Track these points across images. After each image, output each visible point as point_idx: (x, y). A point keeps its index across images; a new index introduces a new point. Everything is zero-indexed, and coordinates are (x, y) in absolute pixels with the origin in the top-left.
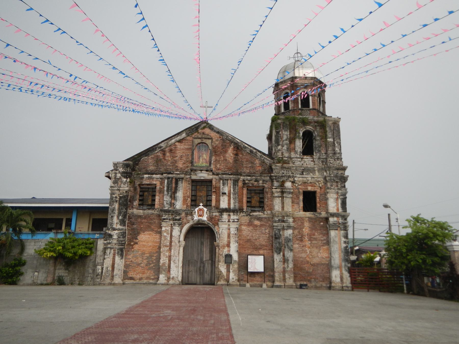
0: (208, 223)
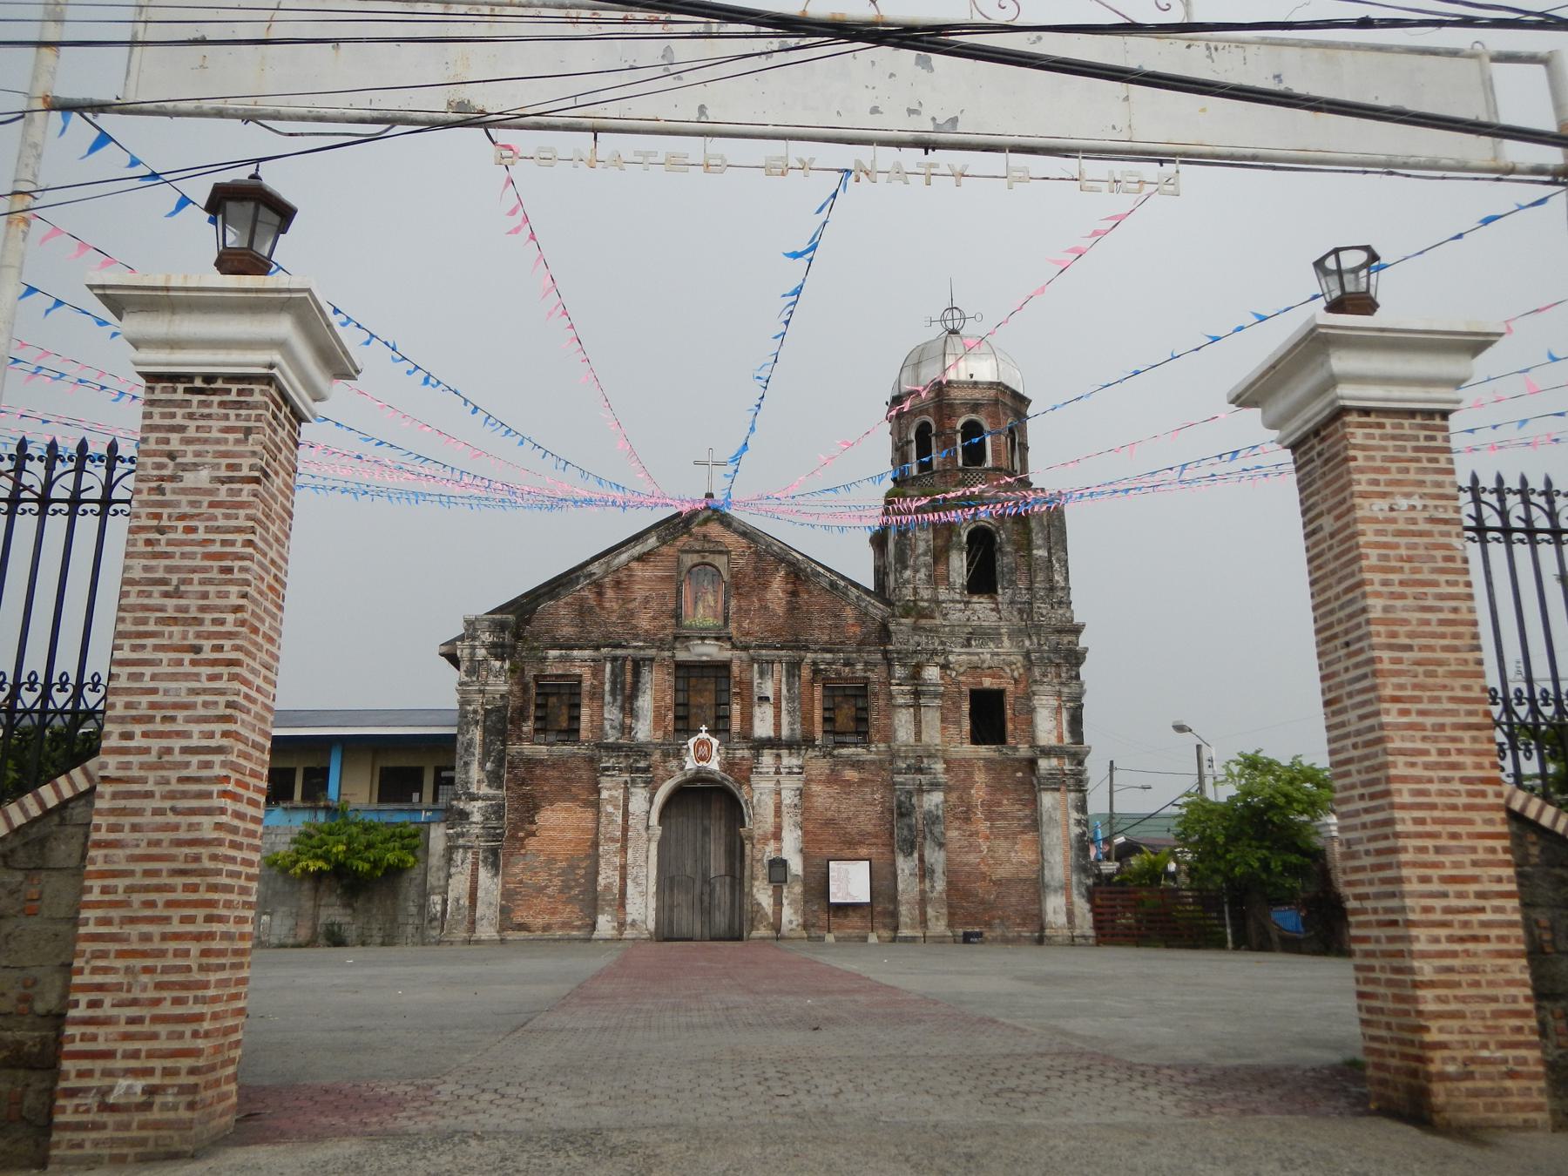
0: (723, 778)
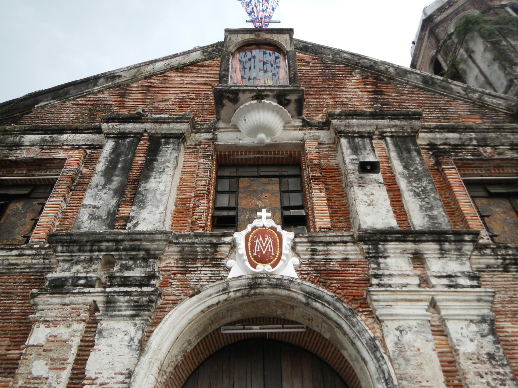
0: (309, 295)
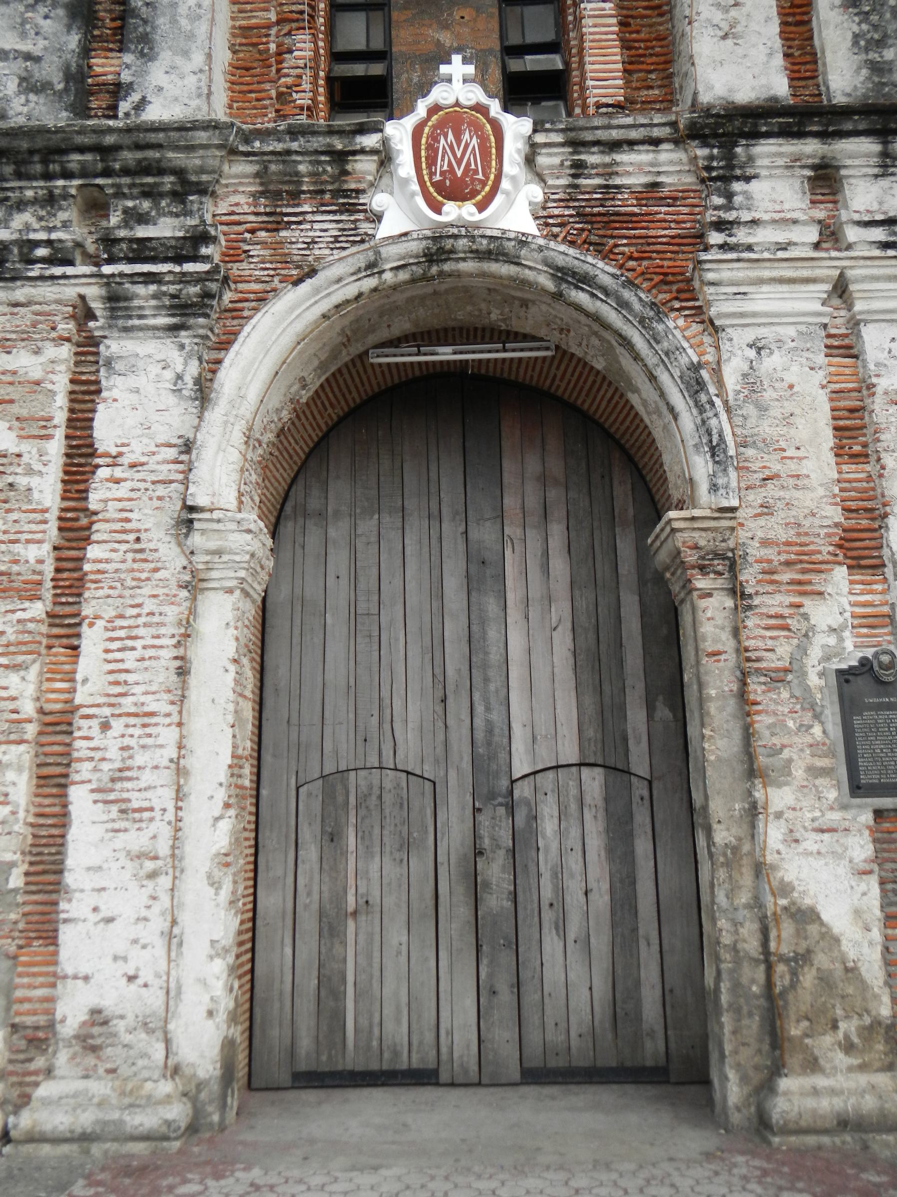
0: (563, 274)
